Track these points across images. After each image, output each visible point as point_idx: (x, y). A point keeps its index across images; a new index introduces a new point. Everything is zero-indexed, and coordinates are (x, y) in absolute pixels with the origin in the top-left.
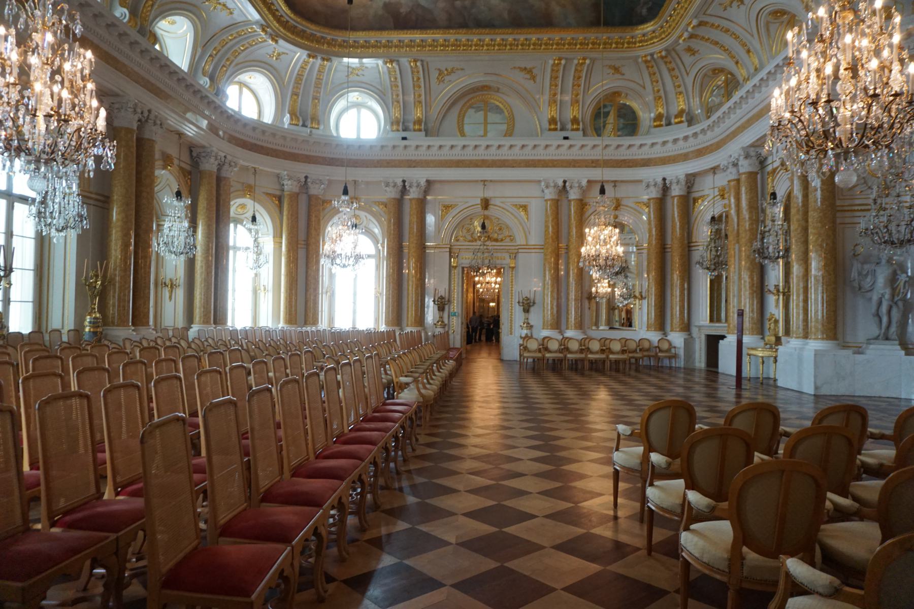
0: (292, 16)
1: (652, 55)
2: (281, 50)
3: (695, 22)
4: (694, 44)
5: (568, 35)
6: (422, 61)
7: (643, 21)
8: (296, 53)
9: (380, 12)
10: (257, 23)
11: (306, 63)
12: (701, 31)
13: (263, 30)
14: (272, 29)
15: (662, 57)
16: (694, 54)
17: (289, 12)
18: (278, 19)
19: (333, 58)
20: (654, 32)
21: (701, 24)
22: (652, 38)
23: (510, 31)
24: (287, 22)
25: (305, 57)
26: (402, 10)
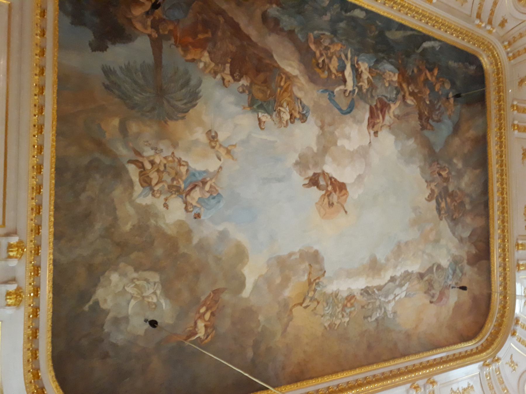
0: (477, 340)
1: (508, 53)
2: (508, 359)
3: (477, 22)
4: (497, 21)
5: (493, 122)
6: (517, 239)
7: (480, 67)
8: (511, 347)
9: (476, 269)
10: (481, 368)
11: (520, 340)
12: (485, 16)
13: (488, 365)
14: (487, 359)
15: (510, 44)
16: (506, 21)
17: (474, 342)
18: (479, 351)
19: (515, 316)
20: (488, 56)
21: (479, 16)
22: (494, 56)
23: (489, 166)
24: (482, 345)
25: (515, 339)
26: (474, 252)
